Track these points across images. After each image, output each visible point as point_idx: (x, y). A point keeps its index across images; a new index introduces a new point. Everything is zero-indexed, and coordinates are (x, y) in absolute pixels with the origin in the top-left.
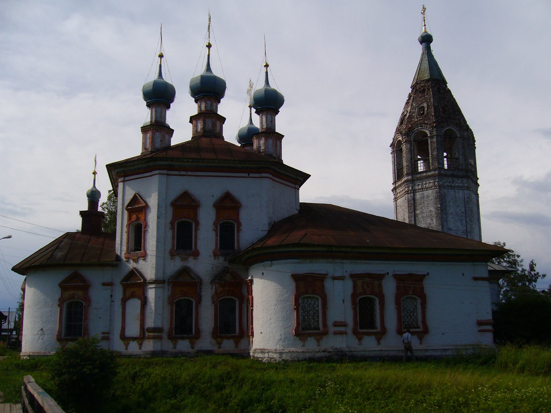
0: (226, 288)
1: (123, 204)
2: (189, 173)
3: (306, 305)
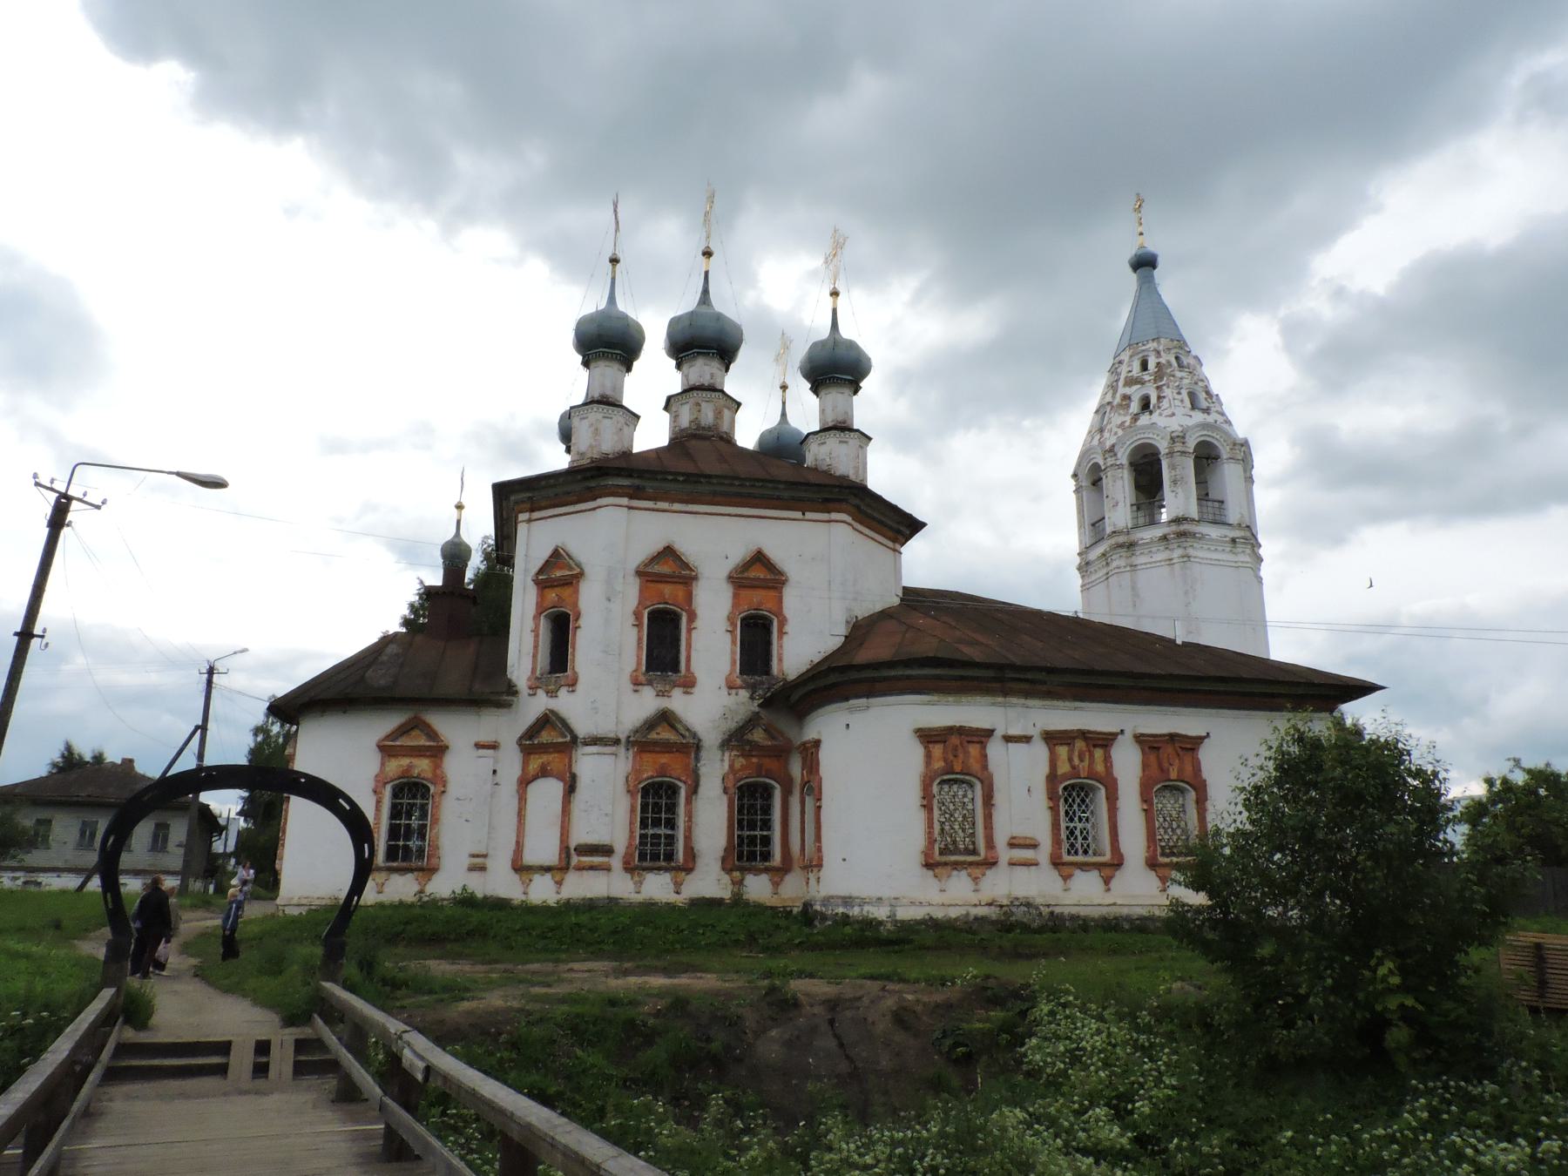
0: (754, 760)
1: (526, 570)
2: (677, 506)
3: (947, 797)
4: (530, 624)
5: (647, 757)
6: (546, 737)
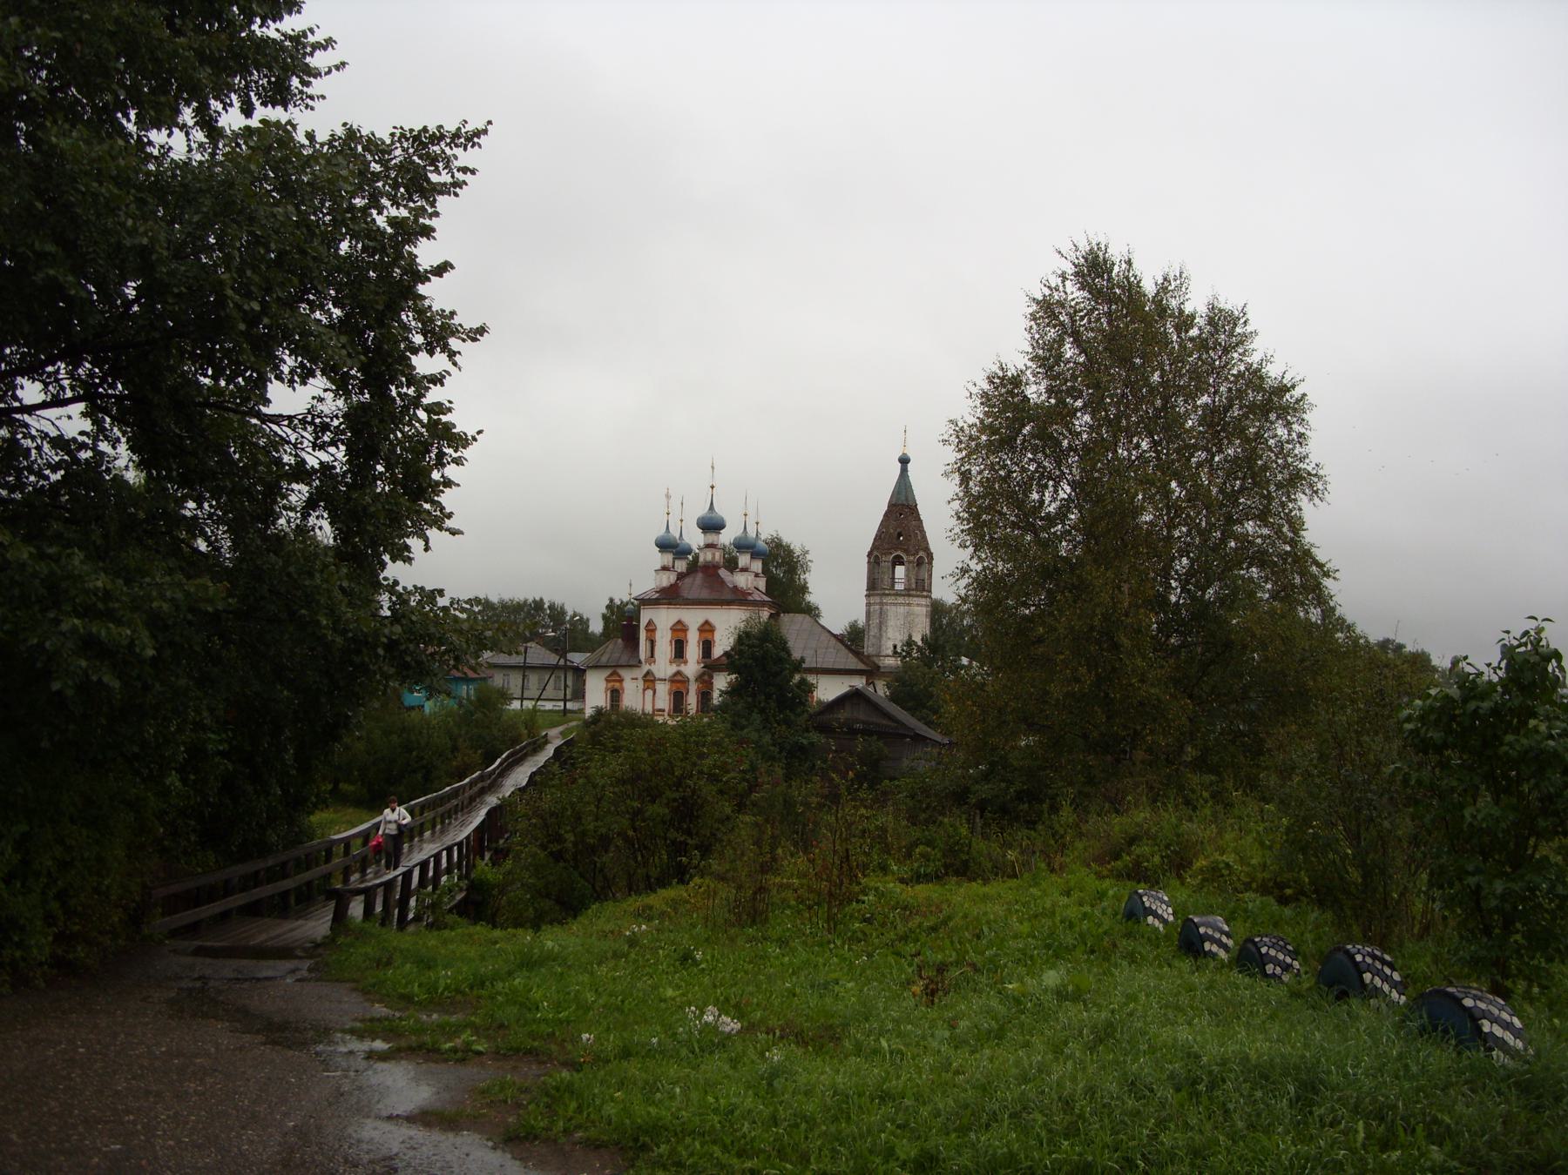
6: (648, 678)
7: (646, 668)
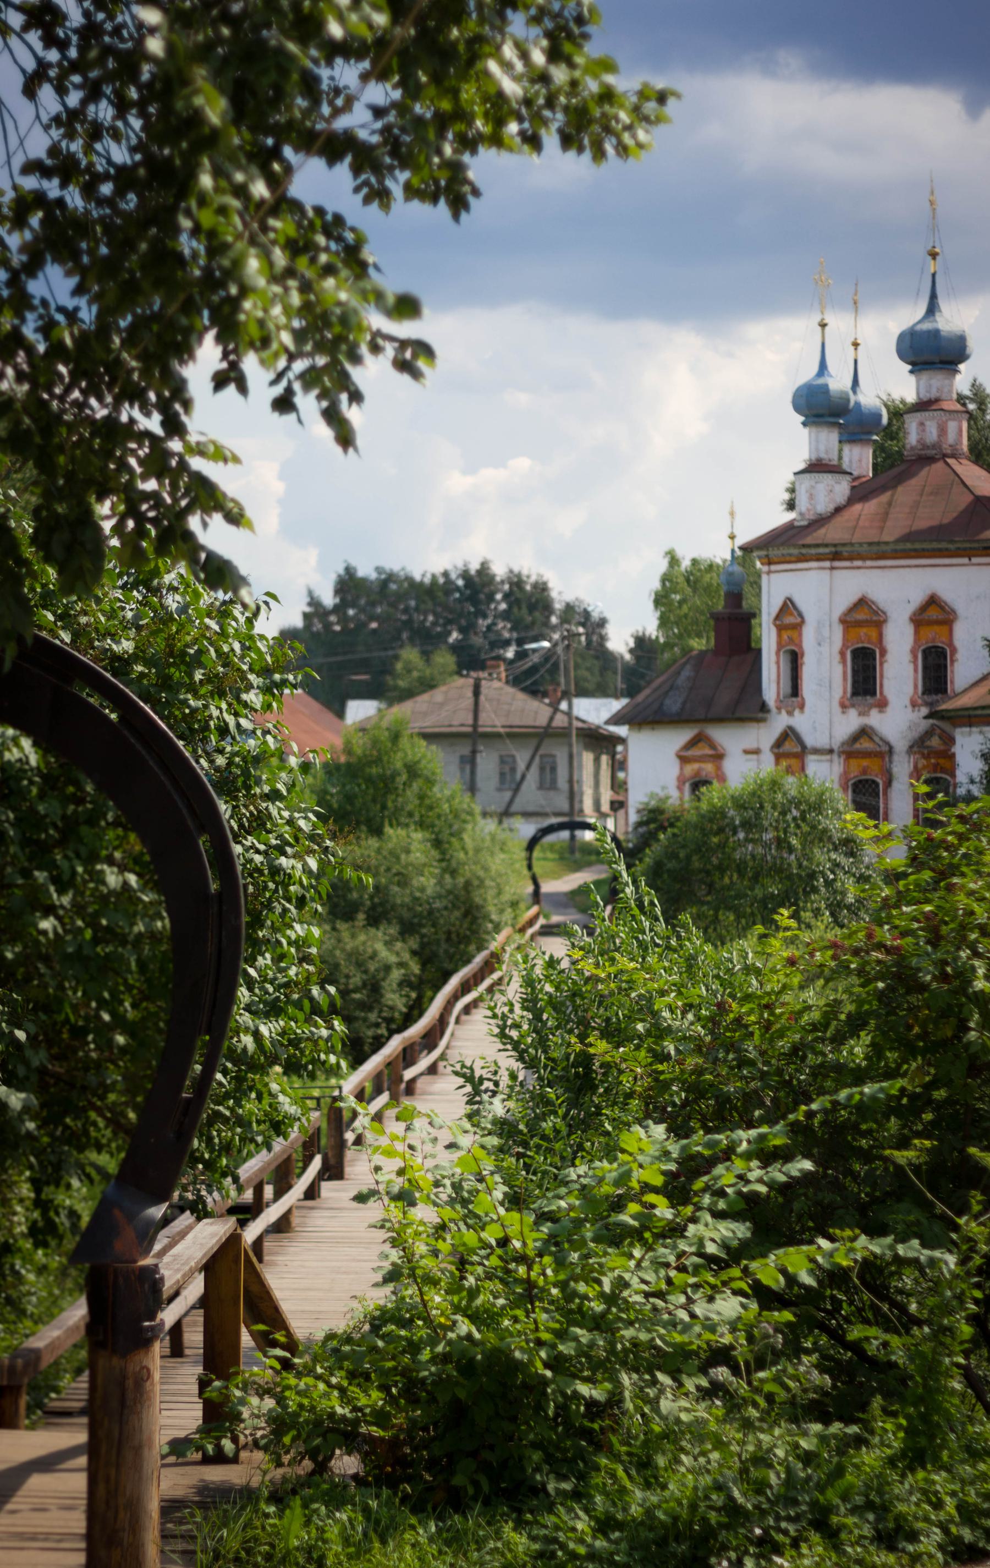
2: (869, 563)
4: (774, 658)
5: (853, 762)
6: (788, 747)
7: (779, 722)
